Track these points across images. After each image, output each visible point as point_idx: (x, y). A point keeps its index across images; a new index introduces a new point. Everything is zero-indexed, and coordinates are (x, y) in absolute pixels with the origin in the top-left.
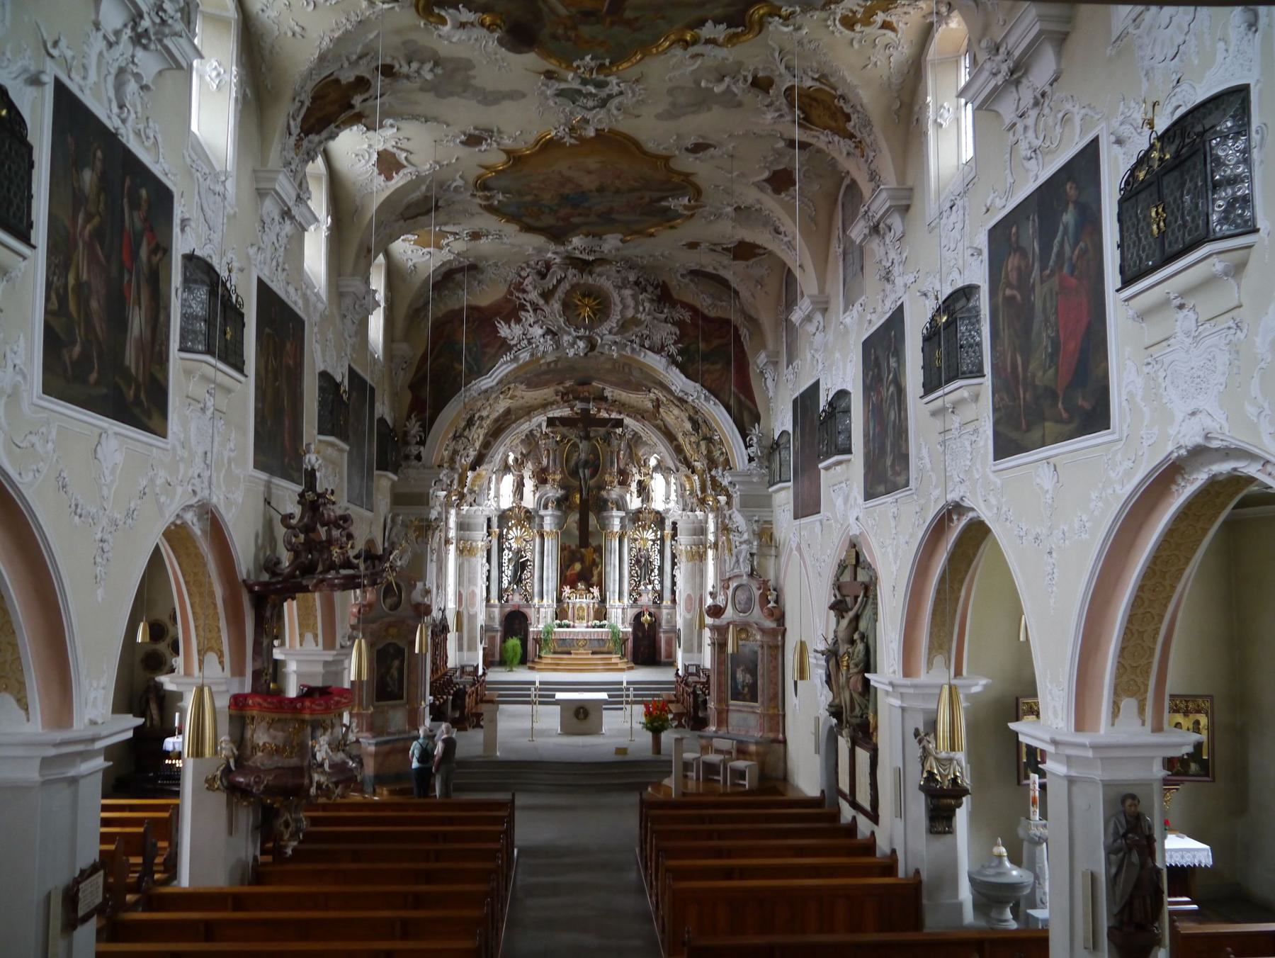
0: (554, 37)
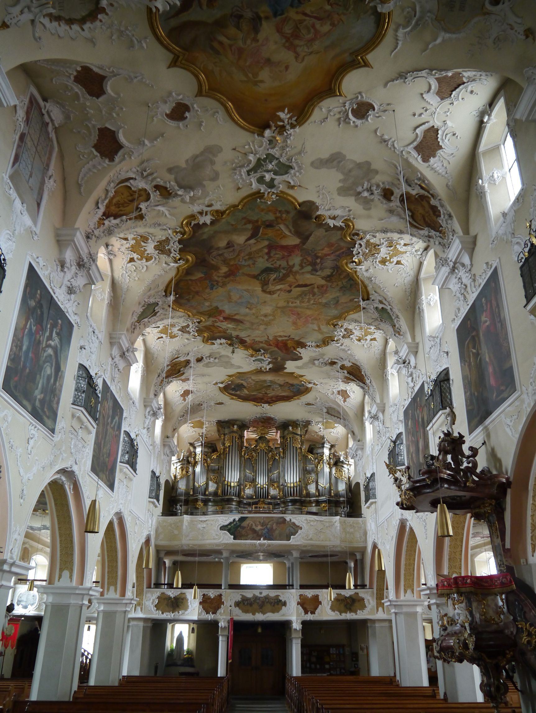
0: (288, 212)
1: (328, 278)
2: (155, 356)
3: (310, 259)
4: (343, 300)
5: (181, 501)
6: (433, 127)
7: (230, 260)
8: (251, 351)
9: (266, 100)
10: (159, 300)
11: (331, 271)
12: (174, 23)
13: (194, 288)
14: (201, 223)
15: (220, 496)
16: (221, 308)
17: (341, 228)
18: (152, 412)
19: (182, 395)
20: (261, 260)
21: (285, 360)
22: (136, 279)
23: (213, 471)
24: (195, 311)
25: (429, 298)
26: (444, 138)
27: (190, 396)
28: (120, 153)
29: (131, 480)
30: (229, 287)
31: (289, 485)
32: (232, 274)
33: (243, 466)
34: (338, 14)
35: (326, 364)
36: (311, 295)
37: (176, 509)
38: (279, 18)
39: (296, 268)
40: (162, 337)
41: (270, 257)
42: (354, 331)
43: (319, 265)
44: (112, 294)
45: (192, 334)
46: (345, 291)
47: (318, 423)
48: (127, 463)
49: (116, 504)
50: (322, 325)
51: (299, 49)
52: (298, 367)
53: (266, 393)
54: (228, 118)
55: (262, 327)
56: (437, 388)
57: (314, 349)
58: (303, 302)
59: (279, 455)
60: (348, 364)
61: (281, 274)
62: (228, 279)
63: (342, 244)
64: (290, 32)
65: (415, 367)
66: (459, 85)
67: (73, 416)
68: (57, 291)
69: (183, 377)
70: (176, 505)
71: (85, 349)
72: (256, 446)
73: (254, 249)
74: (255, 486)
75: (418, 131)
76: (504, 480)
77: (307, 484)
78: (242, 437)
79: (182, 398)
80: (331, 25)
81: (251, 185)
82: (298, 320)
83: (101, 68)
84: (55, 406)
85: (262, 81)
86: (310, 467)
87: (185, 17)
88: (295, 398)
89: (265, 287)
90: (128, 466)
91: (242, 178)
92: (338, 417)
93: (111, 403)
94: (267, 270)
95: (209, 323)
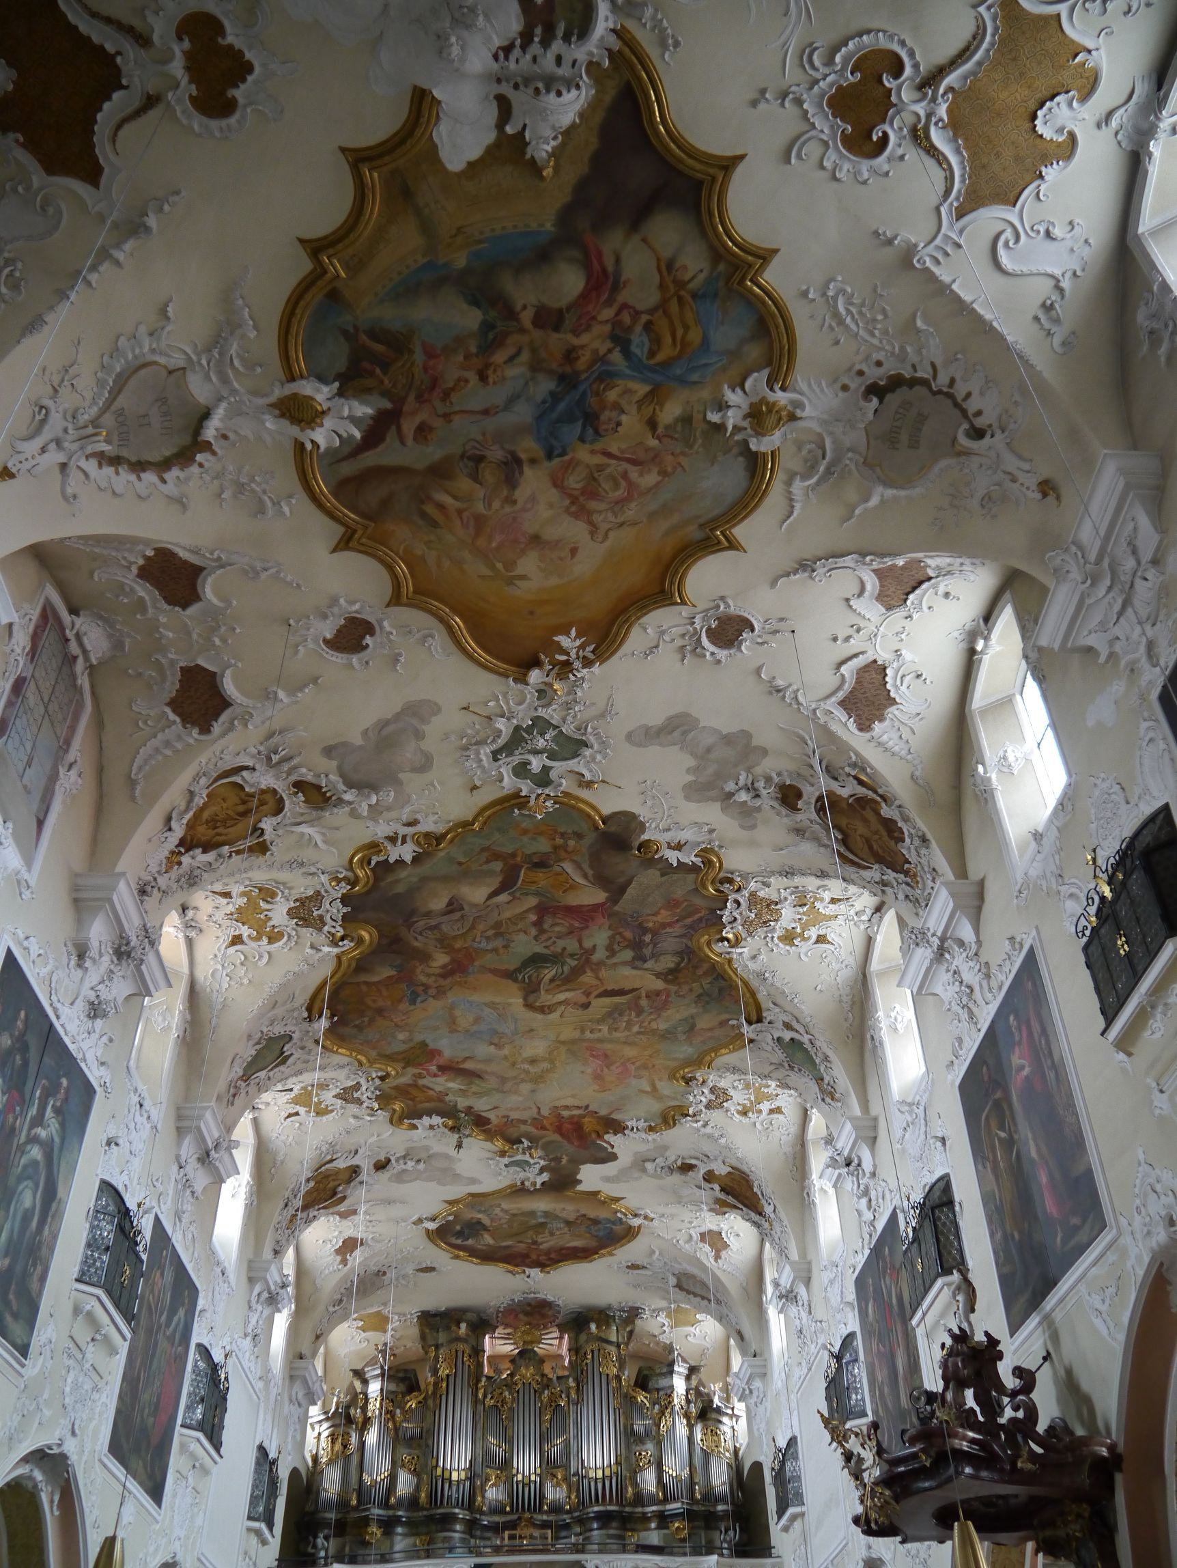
0: (579, 836)
1: (671, 975)
2: (280, 1157)
3: (628, 934)
4: (704, 1022)
5: (328, 1526)
6: (875, 661)
7: (455, 938)
8: (499, 1144)
9: (532, 613)
10: (293, 1029)
11: (676, 959)
12: (348, 469)
13: (374, 1001)
14: (392, 860)
15: (423, 1509)
16: (432, 1046)
17: (694, 868)
18: (265, 1295)
19: (338, 1252)
20: (522, 937)
21: (576, 1162)
22: (245, 981)
23: (410, 1442)
24: (374, 1053)
25: (893, 1014)
26: (898, 683)
27: (358, 1252)
28: (224, 717)
29: (205, 1472)
30: (451, 997)
31: (592, 1474)
32: (458, 968)
33: (480, 1426)
34: (672, 454)
35: (671, 1170)
36: (633, 1014)
37: (315, 1546)
38: (556, 461)
39: (600, 955)
40: (297, 1114)
41: (542, 931)
42: (731, 1092)
43: (651, 946)
44: (189, 1017)
45: (365, 1105)
46: (708, 1003)
47: (656, 1311)
48: (200, 1427)
49: (164, 1540)
50: (660, 1080)
51: (597, 518)
52: (608, 1179)
53: (535, 1243)
54: (452, 647)
55: (526, 1088)
56: (927, 1223)
57: (643, 1135)
58: (616, 1030)
59: (568, 1396)
60: (721, 1170)
61: (566, 969)
62: (449, 980)
63: (699, 902)
64: (578, 486)
65: (873, 1175)
66: (921, 583)
67: (77, 1310)
68: (65, 1011)
69: (342, 1208)
70: (316, 1537)
71: (117, 1144)
72: (511, 1375)
73: (507, 914)
74: (510, 1479)
75: (844, 669)
76: (1104, 1452)
77: (635, 1472)
78: (478, 1351)
79: (339, 1258)
80: (659, 473)
81: (501, 781)
82: (605, 1070)
83: (195, 552)
84: (34, 1286)
85: (523, 577)
86: (641, 1425)
87: (370, 459)
88: (604, 1251)
89: (531, 998)
90: (200, 1435)
91: (481, 767)
92: (703, 1298)
93: (169, 1275)
94: (536, 960)
95: (405, 1079)
